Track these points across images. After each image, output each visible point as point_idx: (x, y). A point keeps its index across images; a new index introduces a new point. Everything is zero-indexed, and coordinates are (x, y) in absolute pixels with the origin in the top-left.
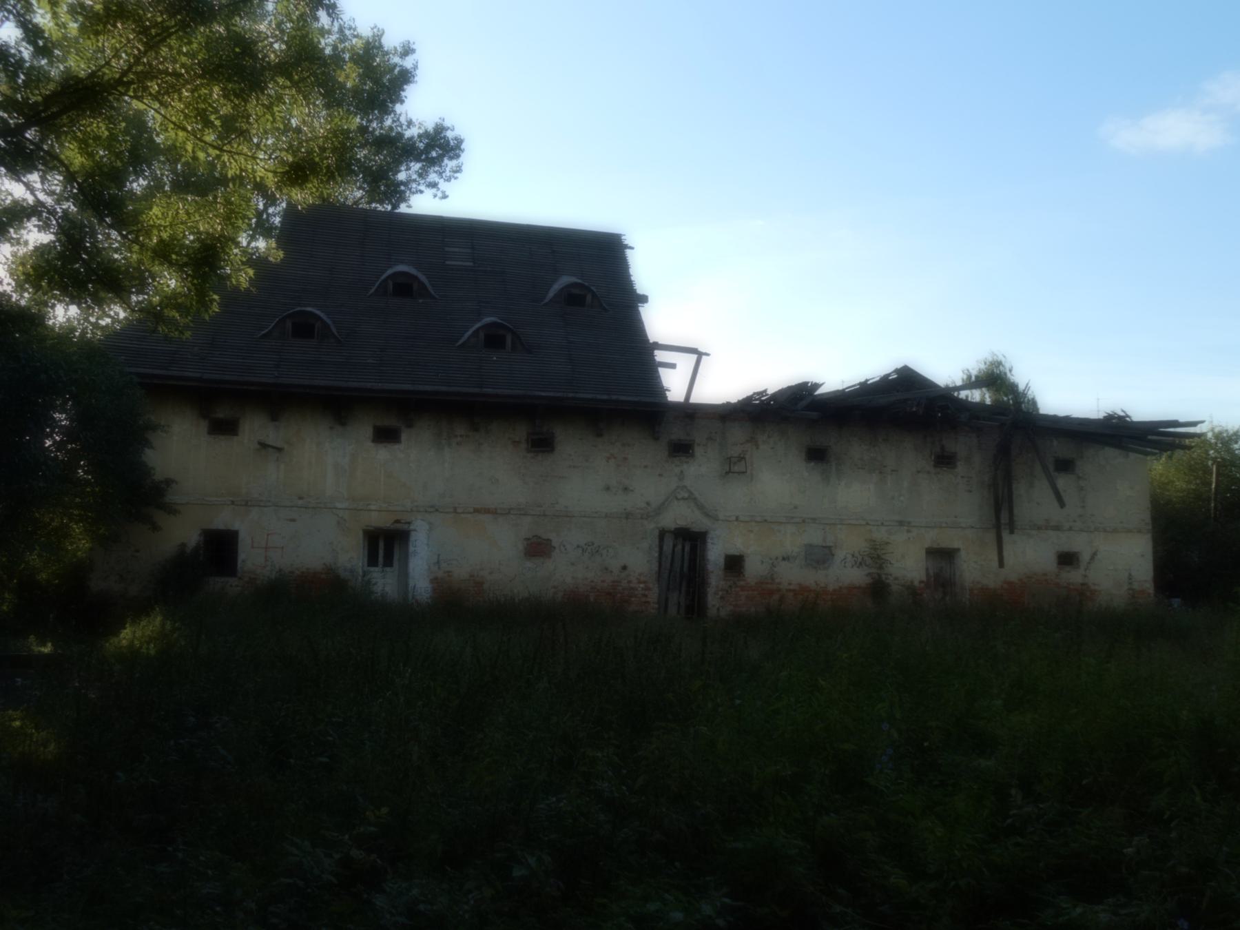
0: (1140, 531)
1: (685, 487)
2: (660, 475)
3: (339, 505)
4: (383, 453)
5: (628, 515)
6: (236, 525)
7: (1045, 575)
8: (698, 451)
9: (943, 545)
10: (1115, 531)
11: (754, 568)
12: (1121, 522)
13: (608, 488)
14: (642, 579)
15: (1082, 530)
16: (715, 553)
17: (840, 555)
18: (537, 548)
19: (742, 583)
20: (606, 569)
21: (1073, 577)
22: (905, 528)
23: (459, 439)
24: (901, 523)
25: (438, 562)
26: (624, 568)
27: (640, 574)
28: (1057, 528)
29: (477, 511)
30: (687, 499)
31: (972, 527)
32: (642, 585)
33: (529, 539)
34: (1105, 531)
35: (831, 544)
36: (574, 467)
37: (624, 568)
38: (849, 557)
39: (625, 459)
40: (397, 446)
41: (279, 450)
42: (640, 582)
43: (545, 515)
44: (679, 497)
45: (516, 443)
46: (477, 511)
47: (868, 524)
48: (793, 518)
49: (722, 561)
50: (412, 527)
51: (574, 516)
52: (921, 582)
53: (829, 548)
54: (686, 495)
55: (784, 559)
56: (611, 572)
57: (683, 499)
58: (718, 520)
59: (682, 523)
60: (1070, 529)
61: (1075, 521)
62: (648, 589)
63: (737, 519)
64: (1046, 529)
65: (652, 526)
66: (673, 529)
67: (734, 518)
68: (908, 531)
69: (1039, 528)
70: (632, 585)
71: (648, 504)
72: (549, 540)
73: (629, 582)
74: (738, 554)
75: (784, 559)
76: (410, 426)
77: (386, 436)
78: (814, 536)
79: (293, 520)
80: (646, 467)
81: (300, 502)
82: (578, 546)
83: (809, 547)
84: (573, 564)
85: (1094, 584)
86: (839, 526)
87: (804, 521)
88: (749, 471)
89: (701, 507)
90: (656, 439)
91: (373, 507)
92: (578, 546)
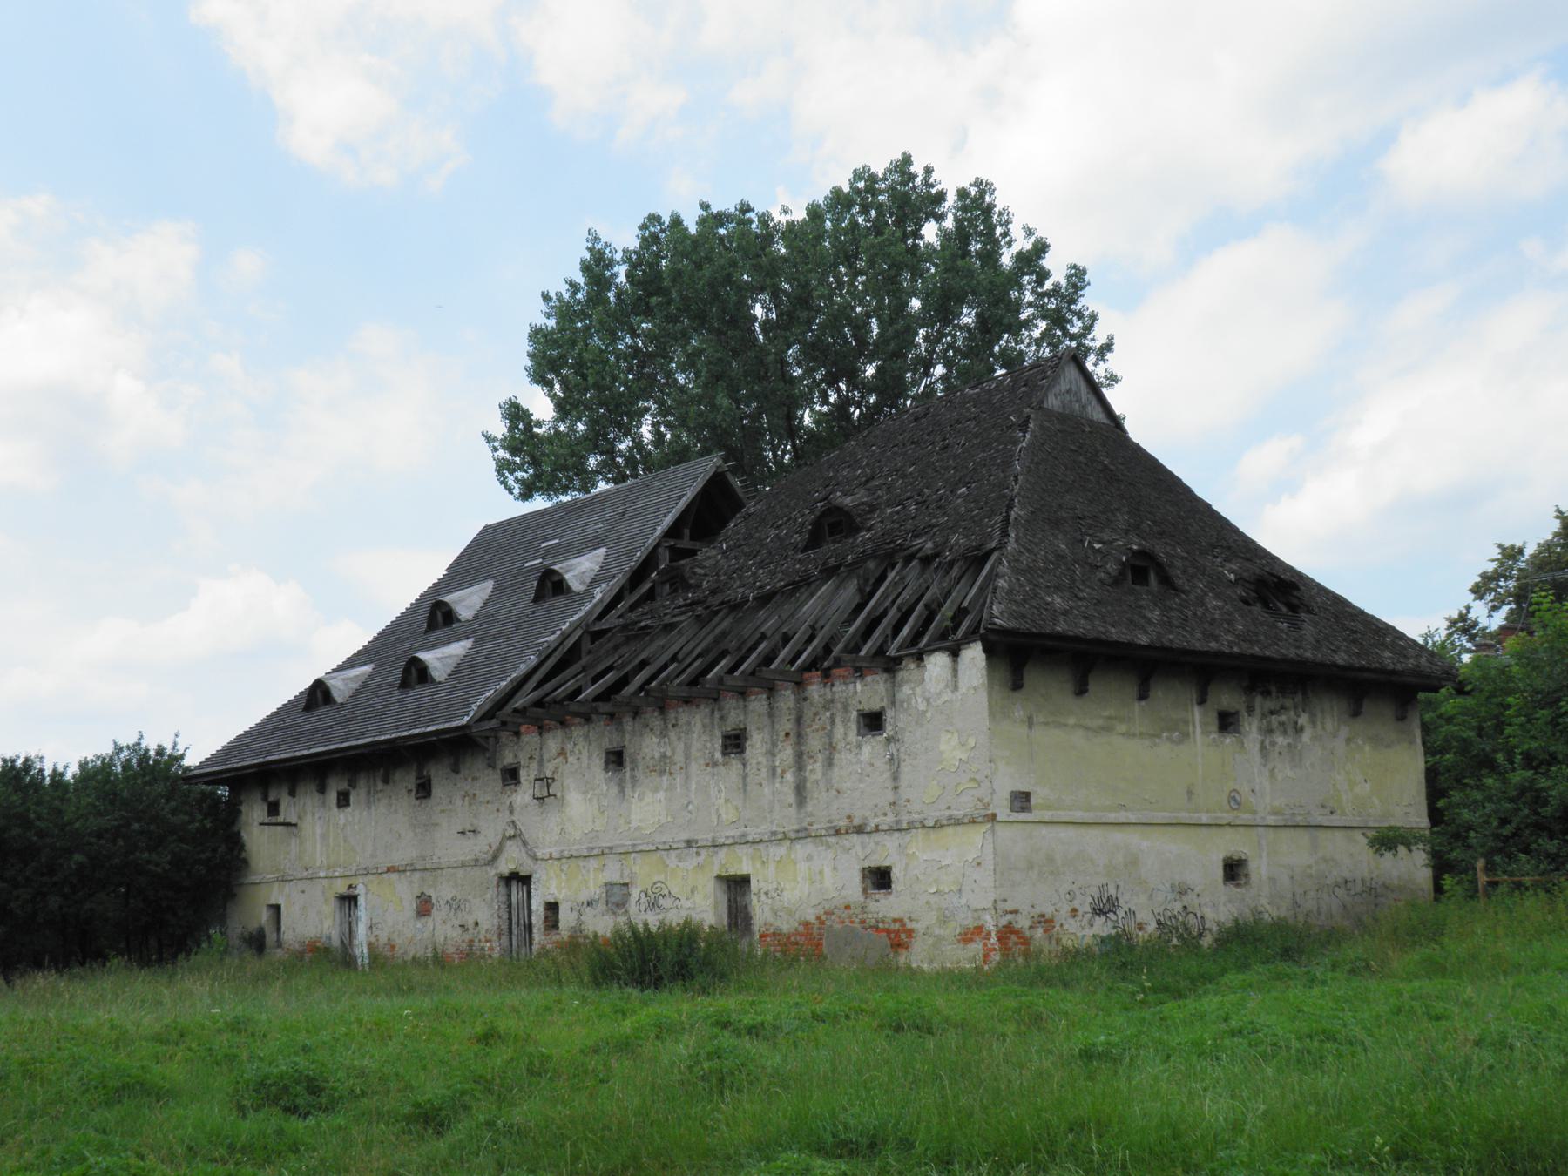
0: (974, 822)
1: (513, 822)
2: (498, 810)
3: (322, 874)
4: (342, 817)
5: (476, 863)
6: (281, 901)
7: (848, 907)
8: (523, 773)
9: (732, 872)
10: (938, 826)
11: (566, 918)
12: (949, 808)
13: (463, 833)
14: (488, 936)
15: (891, 830)
16: (537, 905)
17: (635, 893)
18: (424, 907)
19: (558, 937)
20: (462, 926)
21: (886, 907)
22: (695, 850)
23: (380, 795)
24: (689, 843)
25: (371, 927)
26: (477, 924)
27: (487, 930)
28: (860, 830)
29: (389, 870)
30: (514, 836)
31: (761, 841)
32: (488, 944)
33: (418, 897)
34: (924, 826)
35: (627, 881)
36: (443, 811)
37: (477, 924)
38: (643, 895)
39: (474, 795)
40: (349, 810)
41: (295, 825)
42: (487, 941)
43: (426, 869)
44: (507, 835)
45: (409, 791)
46: (389, 870)
47: (658, 849)
48: (593, 849)
49: (542, 909)
50: (357, 892)
51: (442, 869)
52: (711, 927)
53: (626, 885)
54: (512, 832)
55: (589, 904)
56: (468, 929)
57: (510, 838)
58: (537, 860)
59: (512, 867)
60: (877, 829)
61: (885, 815)
62: (491, 949)
63: (551, 858)
64: (847, 833)
65: (493, 872)
66: (507, 875)
67: (548, 856)
68: (698, 854)
69: (837, 832)
70: (482, 944)
71: (490, 847)
72: (430, 896)
73: (480, 941)
74: (552, 900)
75: (589, 904)
76: (354, 787)
77: (343, 800)
78: (613, 873)
79: (303, 892)
80: (488, 802)
81: (305, 874)
82: (448, 902)
83: (609, 885)
84: (444, 922)
85: (911, 919)
86: (633, 855)
87: (603, 854)
88: (559, 795)
89: (525, 843)
90: (492, 766)
91: (337, 874)
92: (448, 902)
